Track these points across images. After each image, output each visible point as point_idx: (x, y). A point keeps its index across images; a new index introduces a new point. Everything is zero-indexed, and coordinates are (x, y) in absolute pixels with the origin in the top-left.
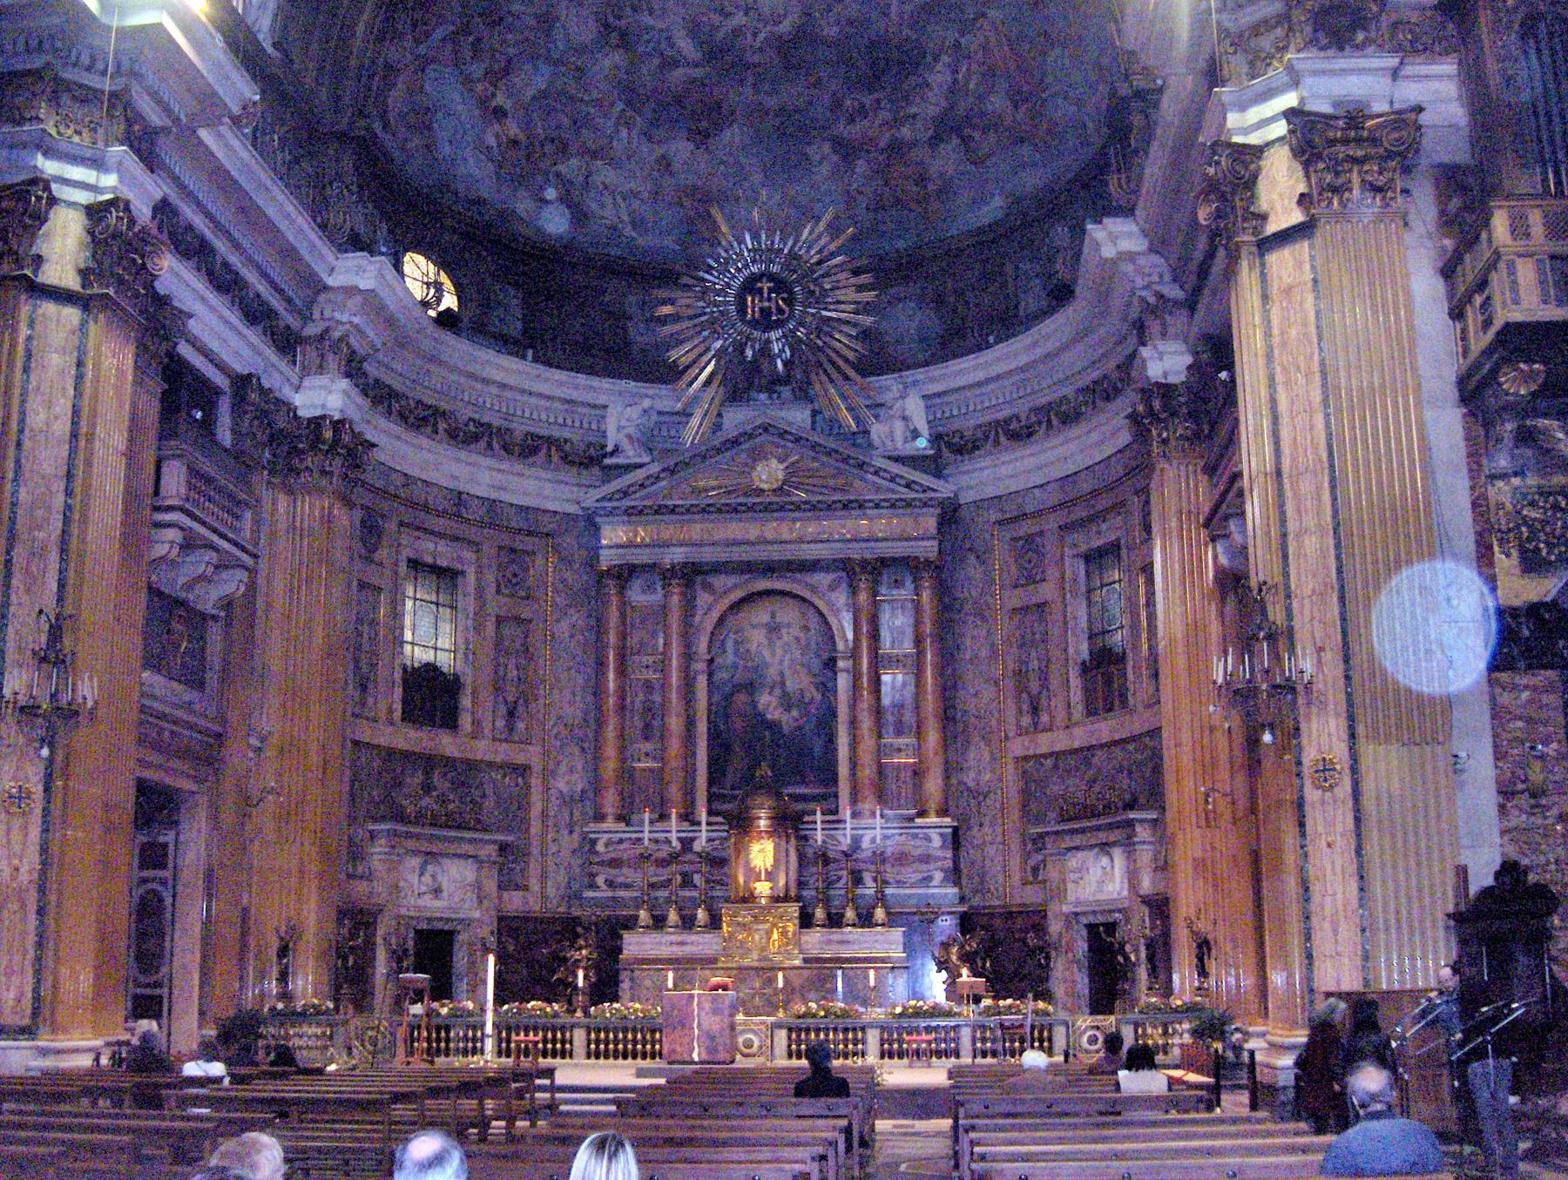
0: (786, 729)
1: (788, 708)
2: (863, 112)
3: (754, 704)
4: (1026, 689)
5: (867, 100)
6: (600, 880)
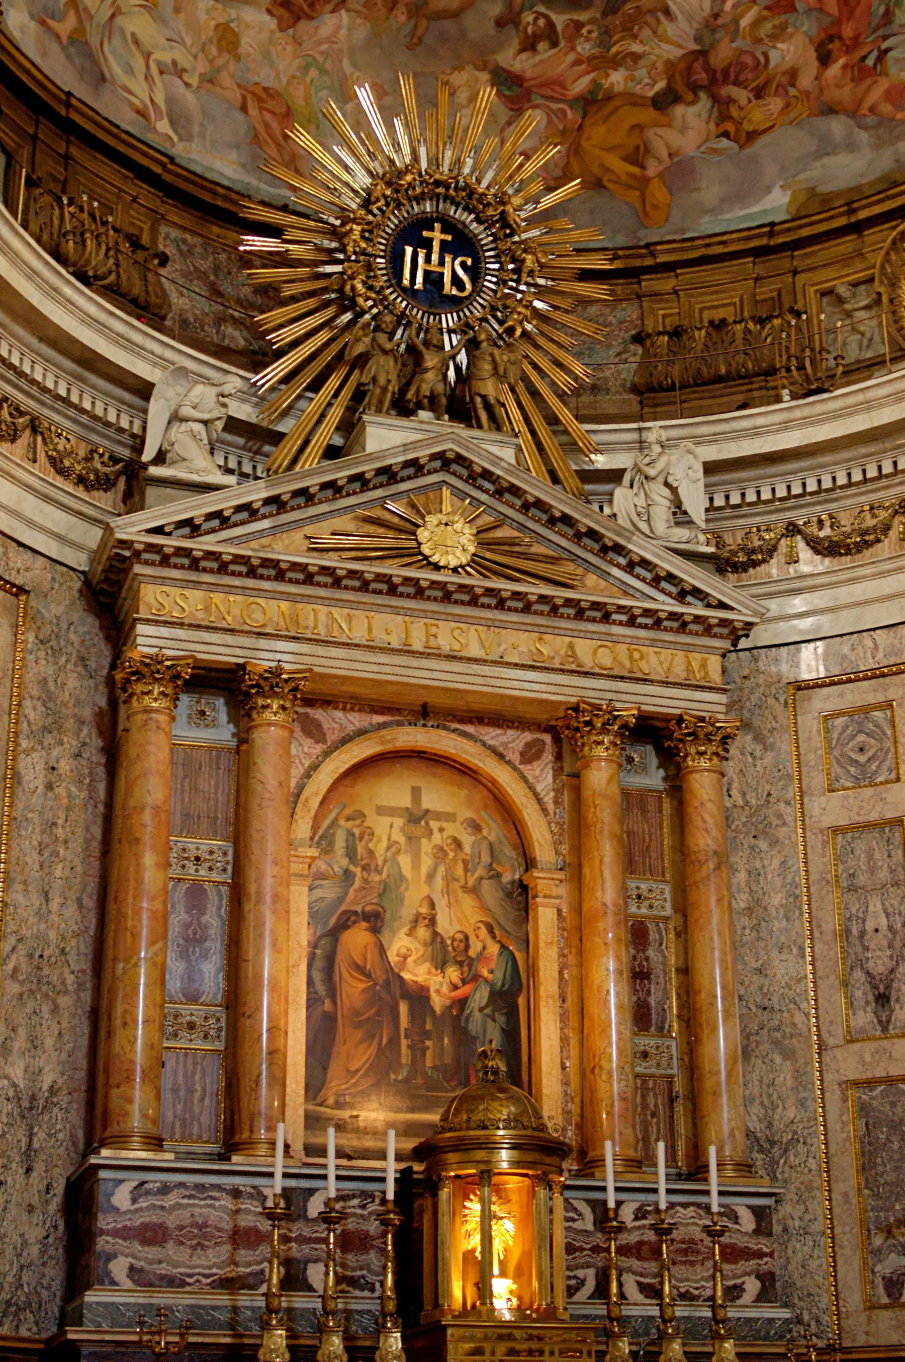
0: (438, 1003)
1: (441, 965)
2: (551, 35)
3: (382, 951)
4: (860, 963)
5: (560, 20)
6: (119, 1268)
